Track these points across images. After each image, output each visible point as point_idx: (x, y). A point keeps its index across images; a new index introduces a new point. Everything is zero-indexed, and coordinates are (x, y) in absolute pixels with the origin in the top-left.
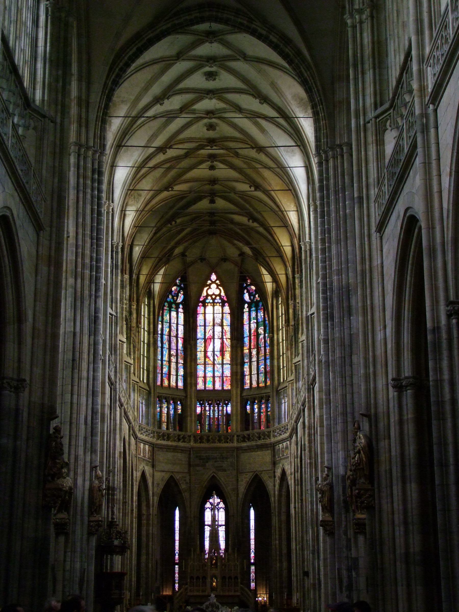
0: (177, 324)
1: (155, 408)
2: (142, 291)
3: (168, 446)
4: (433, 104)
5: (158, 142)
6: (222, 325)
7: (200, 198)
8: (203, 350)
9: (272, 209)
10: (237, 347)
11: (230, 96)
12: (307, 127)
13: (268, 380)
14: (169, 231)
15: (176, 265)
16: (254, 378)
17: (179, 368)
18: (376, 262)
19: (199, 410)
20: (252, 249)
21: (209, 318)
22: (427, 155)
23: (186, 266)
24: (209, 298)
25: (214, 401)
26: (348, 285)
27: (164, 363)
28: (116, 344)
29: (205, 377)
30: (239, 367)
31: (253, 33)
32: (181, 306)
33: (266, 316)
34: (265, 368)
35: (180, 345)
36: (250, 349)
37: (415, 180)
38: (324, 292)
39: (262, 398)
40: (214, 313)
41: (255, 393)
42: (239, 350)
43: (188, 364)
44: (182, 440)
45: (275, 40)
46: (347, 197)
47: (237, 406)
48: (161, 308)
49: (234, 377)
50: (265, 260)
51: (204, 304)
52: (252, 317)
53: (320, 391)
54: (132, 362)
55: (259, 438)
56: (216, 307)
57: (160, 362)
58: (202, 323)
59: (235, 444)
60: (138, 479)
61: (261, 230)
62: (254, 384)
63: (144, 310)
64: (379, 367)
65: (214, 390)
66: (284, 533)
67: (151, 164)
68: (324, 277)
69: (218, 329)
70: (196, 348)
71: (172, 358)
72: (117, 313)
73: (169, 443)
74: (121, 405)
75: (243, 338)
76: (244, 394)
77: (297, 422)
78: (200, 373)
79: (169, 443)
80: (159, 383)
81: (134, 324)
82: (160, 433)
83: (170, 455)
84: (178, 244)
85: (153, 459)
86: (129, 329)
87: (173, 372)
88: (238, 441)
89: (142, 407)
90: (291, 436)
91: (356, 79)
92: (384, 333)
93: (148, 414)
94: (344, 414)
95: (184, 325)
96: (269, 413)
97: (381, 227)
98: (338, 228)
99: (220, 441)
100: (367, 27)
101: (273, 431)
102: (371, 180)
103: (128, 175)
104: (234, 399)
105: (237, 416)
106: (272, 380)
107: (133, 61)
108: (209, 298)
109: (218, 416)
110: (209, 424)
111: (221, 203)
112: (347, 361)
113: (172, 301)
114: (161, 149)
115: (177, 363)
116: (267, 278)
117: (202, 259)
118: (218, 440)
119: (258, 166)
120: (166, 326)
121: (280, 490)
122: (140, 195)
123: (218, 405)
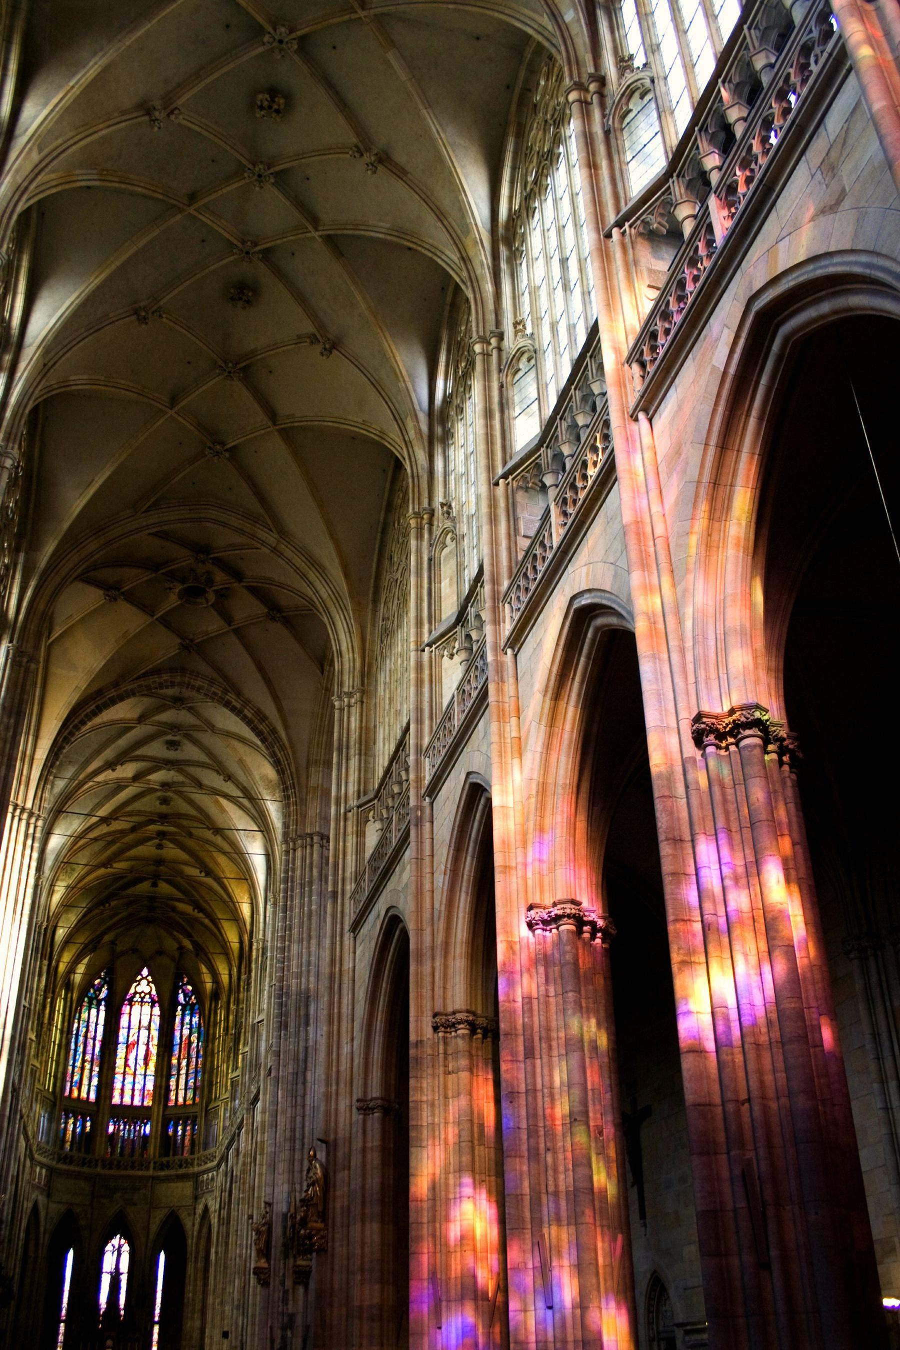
0: (97, 1024)
1: (59, 1124)
2: (60, 982)
4: (430, 796)
5: (103, 812)
6: (149, 1028)
7: (140, 880)
9: (221, 898)
11: (192, 770)
12: (273, 810)
14: (101, 913)
15: (103, 954)
16: (181, 1094)
18: (348, 965)
19: (111, 1129)
20: (195, 943)
22: (420, 849)
23: (114, 956)
26: (308, 990)
28: (25, 1043)
29: (122, 1089)
31: (227, 705)
34: (195, 1083)
36: (179, 1059)
37: (404, 874)
38: (280, 996)
39: (188, 1118)
45: (249, 715)
46: (314, 892)
48: (80, 1004)
50: (206, 955)
51: (131, 1003)
53: (263, 1112)
54: (38, 1065)
55: (180, 1166)
59: (151, 1173)
60: (29, 1211)
61: (206, 921)
62: (181, 1100)
63: (60, 1005)
64: (342, 1085)
65: (132, 1106)
66: (200, 1283)
67: (92, 835)
68: (281, 979)
69: (144, 1033)
70: (116, 1055)
72: (30, 1004)
73: (72, 1168)
74: (22, 1117)
77: (228, 1148)
78: (118, 1085)
79: (72, 1168)
80: (67, 1093)
81: (46, 1020)
84: (109, 929)
86: (40, 1024)
87: (85, 1081)
88: (154, 1168)
90: (219, 1166)
91: (339, 764)
92: (351, 1047)
94: (293, 1139)
97: (356, 926)
98: (301, 925)
99: (133, 1167)
100: (355, 712)
102: (348, 874)
103: (64, 845)
105: (156, 1138)
106: (202, 1098)
107: (90, 719)
110: (122, 1148)
111: (164, 888)
112: (300, 1079)
114: (104, 820)
115: (91, 1070)
116: (207, 978)
117: (135, 951)
119: (212, 849)
121: (200, 1231)
122: (73, 870)
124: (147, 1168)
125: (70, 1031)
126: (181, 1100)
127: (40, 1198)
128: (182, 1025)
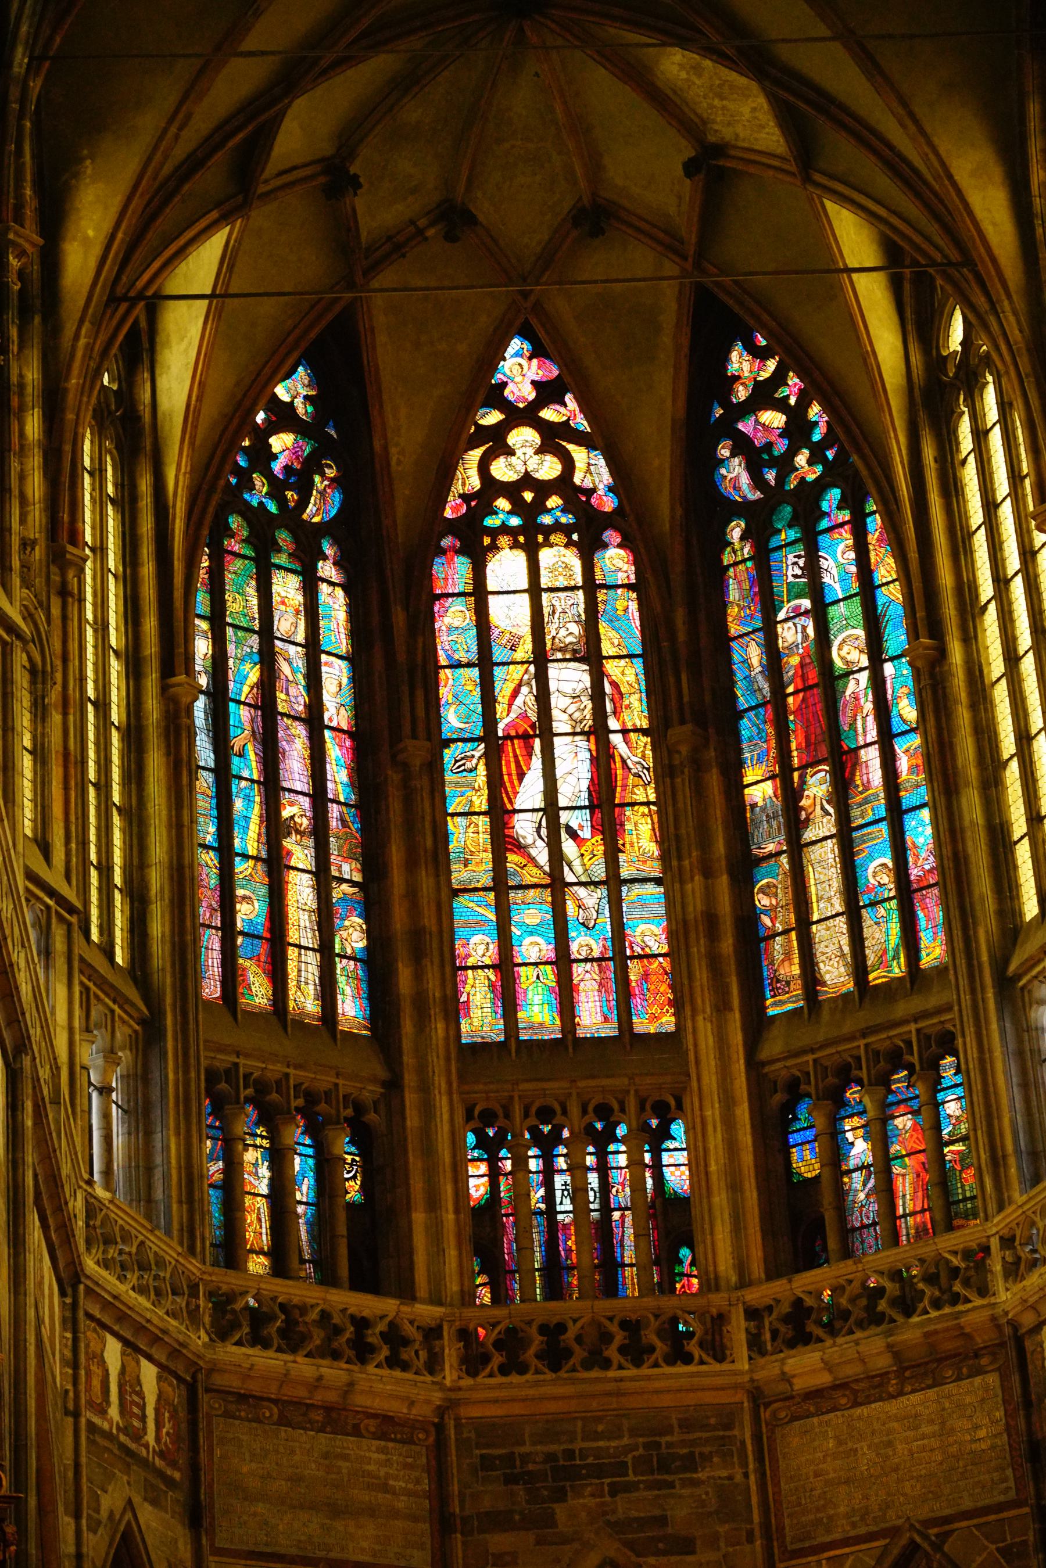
0: (313, 648)
6: (590, 654)
8: (481, 802)
10: (698, 766)
16: (831, 940)
17: (340, 909)
21: (510, 615)
23: (355, 258)
24: (503, 504)
25: (575, 1110)
27: (241, 867)
30: (723, 881)
32: (328, 549)
35: (338, 776)
40: (535, 590)
41: (848, 1027)
42: (714, 780)
43: (397, 879)
44: (385, 1352)
47: (729, 1122)
49: (699, 948)
52: (780, 588)
55: (907, 1305)
56: (546, 556)
57: (209, 859)
58: (466, 647)
62: (835, 974)
69: (568, 679)
75: (740, 715)
76: (773, 1047)
78: (478, 946)
82: (231, 1297)
83: (305, 1449)
85: (194, 1469)
88: (755, 1344)
89: (106, 1116)
93: (149, 1170)
95: (357, 659)
99: (636, 1353)
101: (1008, 1242)
104: (710, 1080)
105: (735, 1187)
108: (503, 504)
109: (606, 1209)
117: (454, 218)
118: (622, 1350)
120: (241, 649)
124: (717, 1349)
126: (835, 974)
127: (148, 1516)
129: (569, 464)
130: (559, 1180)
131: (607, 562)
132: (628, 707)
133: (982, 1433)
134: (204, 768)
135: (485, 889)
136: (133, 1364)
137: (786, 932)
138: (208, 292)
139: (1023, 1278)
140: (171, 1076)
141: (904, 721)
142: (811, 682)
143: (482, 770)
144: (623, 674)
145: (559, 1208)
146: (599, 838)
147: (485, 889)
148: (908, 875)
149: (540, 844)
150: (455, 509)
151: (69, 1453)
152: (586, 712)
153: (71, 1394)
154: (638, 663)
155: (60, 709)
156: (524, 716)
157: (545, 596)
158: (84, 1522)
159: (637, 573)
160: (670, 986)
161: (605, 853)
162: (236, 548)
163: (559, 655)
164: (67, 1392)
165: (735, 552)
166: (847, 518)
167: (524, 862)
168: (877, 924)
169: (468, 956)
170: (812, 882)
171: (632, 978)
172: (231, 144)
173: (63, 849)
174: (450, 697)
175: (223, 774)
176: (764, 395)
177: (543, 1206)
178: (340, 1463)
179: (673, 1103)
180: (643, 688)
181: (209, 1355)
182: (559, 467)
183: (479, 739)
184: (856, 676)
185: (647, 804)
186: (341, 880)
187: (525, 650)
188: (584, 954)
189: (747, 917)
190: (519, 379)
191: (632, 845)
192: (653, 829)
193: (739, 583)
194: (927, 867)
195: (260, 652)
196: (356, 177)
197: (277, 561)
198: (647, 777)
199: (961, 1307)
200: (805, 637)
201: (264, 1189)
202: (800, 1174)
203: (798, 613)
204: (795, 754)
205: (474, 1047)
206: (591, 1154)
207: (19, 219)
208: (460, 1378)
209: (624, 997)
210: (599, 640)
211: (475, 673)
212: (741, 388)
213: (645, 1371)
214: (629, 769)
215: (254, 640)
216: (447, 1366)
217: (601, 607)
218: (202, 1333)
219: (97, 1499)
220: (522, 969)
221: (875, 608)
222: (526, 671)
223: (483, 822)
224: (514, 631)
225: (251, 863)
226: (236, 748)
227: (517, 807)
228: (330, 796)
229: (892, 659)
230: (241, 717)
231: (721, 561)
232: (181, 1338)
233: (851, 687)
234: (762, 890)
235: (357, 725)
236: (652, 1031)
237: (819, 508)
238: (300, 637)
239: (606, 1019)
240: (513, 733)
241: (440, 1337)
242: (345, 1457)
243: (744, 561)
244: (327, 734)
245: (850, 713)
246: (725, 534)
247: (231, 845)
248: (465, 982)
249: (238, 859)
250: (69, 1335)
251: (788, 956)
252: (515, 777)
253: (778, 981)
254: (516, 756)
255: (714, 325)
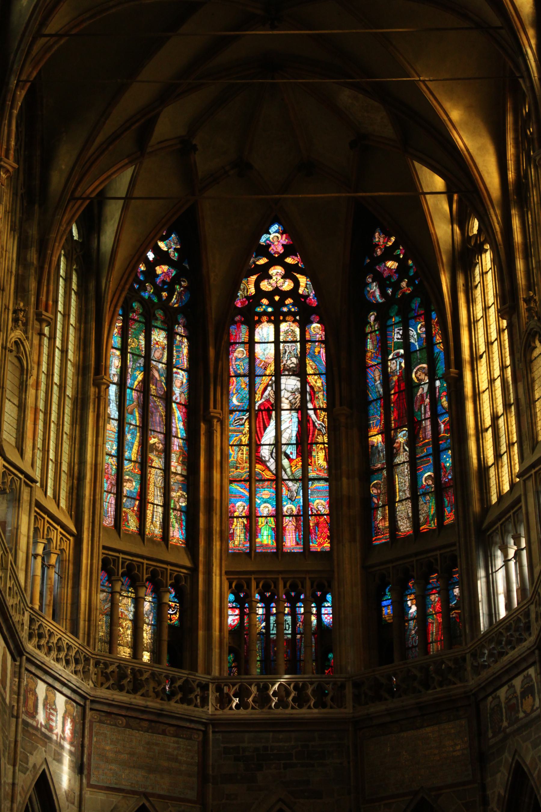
3: (129, 707)
8: (245, 440)
13: (447, 510)
16: (404, 510)
27: (128, 466)
32: (181, 320)
33: (436, 330)
34: (437, 478)
35: (178, 425)
40: (277, 342)
44: (179, 696)
56: (284, 327)
57: (113, 461)
59: (348, 710)
62: (405, 526)
63: (65, 302)
69: (290, 383)
71: (151, 456)
73: (137, 700)
78: (240, 507)
79: (137, 700)
87: (155, 496)
96: (453, 614)
101: (474, 655)
108: (265, 301)
109: (294, 633)
113: (156, 301)
115: (167, 470)
123: (293, 602)
124: (339, 701)
125: (101, 368)
126: (405, 526)
128: (384, 350)
129: (297, 284)
130: (272, 619)
131: (312, 330)
132: (317, 398)
133: (458, 747)
134: (113, 419)
135: (244, 480)
136: (52, 695)
137: (383, 506)
138: (124, 196)
139: (479, 674)
140: (84, 561)
141: (444, 408)
142: (402, 389)
143: (247, 423)
144: (316, 382)
145: (271, 632)
146: (300, 459)
147: (244, 480)
148: (441, 481)
149: (272, 461)
150: (242, 303)
151: (13, 734)
152: (297, 399)
153: (16, 708)
154: (323, 377)
155: (35, 388)
156: (268, 401)
157: (282, 345)
158: (17, 768)
159: (325, 335)
160: (329, 529)
161: (302, 465)
162: (136, 317)
163: (287, 373)
164: (13, 706)
165: (371, 326)
166: (423, 312)
167: (263, 468)
168: (426, 503)
169: (235, 511)
170: (397, 483)
171: (311, 525)
172: (134, 127)
173: (31, 452)
174: (234, 391)
175: (121, 421)
176: (389, 254)
177: (264, 631)
178: (155, 747)
179: (326, 584)
180: (325, 389)
181: (92, 693)
182: (292, 285)
183: (247, 411)
184: (422, 386)
185: (323, 443)
186: (176, 474)
187: (271, 369)
188: (289, 512)
189: (367, 498)
190: (276, 243)
191: (315, 462)
192: (325, 455)
193: (372, 341)
194: (450, 477)
195: (144, 366)
196: (195, 145)
197: (156, 324)
198: (324, 431)
199: (452, 687)
200: (401, 367)
201: (131, 616)
202: (386, 621)
203: (398, 356)
204: (393, 422)
205: (234, 554)
206: (287, 607)
207: (7, 156)
208: (216, 709)
209: (306, 534)
210: (305, 366)
211: (247, 380)
212: (379, 250)
213: (304, 710)
214: (316, 427)
215: (142, 361)
216: (210, 704)
217: (308, 351)
218: (91, 683)
219: (27, 758)
220: (260, 519)
221: (433, 353)
222: (271, 380)
223: (245, 449)
224: (266, 360)
225: (133, 464)
226: (129, 410)
227: (262, 442)
228: (174, 434)
229: (439, 379)
230: (132, 395)
231: (365, 330)
232: (78, 685)
233: (420, 391)
234: (374, 486)
235: (189, 402)
236: (319, 550)
237: (410, 307)
238: (165, 360)
239: (297, 544)
240: (262, 408)
241: (208, 690)
242: (157, 744)
243: (375, 331)
244: (174, 405)
245: (418, 404)
246: (367, 318)
247: (123, 455)
248: (232, 524)
249: (126, 462)
250: (17, 680)
251: (384, 518)
252: (262, 429)
253: (379, 529)
254: (263, 419)
255: (365, 220)
